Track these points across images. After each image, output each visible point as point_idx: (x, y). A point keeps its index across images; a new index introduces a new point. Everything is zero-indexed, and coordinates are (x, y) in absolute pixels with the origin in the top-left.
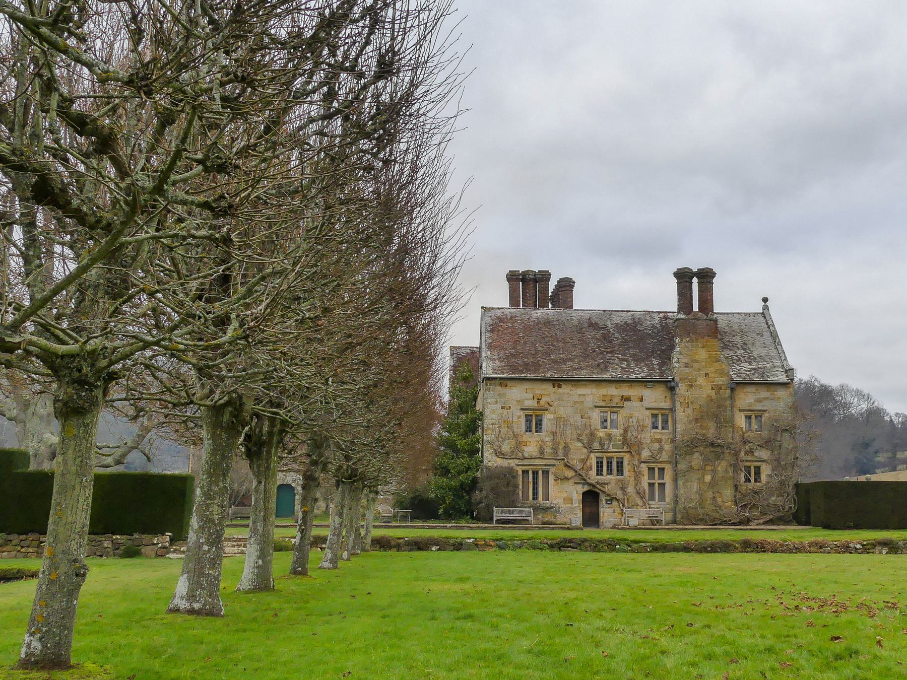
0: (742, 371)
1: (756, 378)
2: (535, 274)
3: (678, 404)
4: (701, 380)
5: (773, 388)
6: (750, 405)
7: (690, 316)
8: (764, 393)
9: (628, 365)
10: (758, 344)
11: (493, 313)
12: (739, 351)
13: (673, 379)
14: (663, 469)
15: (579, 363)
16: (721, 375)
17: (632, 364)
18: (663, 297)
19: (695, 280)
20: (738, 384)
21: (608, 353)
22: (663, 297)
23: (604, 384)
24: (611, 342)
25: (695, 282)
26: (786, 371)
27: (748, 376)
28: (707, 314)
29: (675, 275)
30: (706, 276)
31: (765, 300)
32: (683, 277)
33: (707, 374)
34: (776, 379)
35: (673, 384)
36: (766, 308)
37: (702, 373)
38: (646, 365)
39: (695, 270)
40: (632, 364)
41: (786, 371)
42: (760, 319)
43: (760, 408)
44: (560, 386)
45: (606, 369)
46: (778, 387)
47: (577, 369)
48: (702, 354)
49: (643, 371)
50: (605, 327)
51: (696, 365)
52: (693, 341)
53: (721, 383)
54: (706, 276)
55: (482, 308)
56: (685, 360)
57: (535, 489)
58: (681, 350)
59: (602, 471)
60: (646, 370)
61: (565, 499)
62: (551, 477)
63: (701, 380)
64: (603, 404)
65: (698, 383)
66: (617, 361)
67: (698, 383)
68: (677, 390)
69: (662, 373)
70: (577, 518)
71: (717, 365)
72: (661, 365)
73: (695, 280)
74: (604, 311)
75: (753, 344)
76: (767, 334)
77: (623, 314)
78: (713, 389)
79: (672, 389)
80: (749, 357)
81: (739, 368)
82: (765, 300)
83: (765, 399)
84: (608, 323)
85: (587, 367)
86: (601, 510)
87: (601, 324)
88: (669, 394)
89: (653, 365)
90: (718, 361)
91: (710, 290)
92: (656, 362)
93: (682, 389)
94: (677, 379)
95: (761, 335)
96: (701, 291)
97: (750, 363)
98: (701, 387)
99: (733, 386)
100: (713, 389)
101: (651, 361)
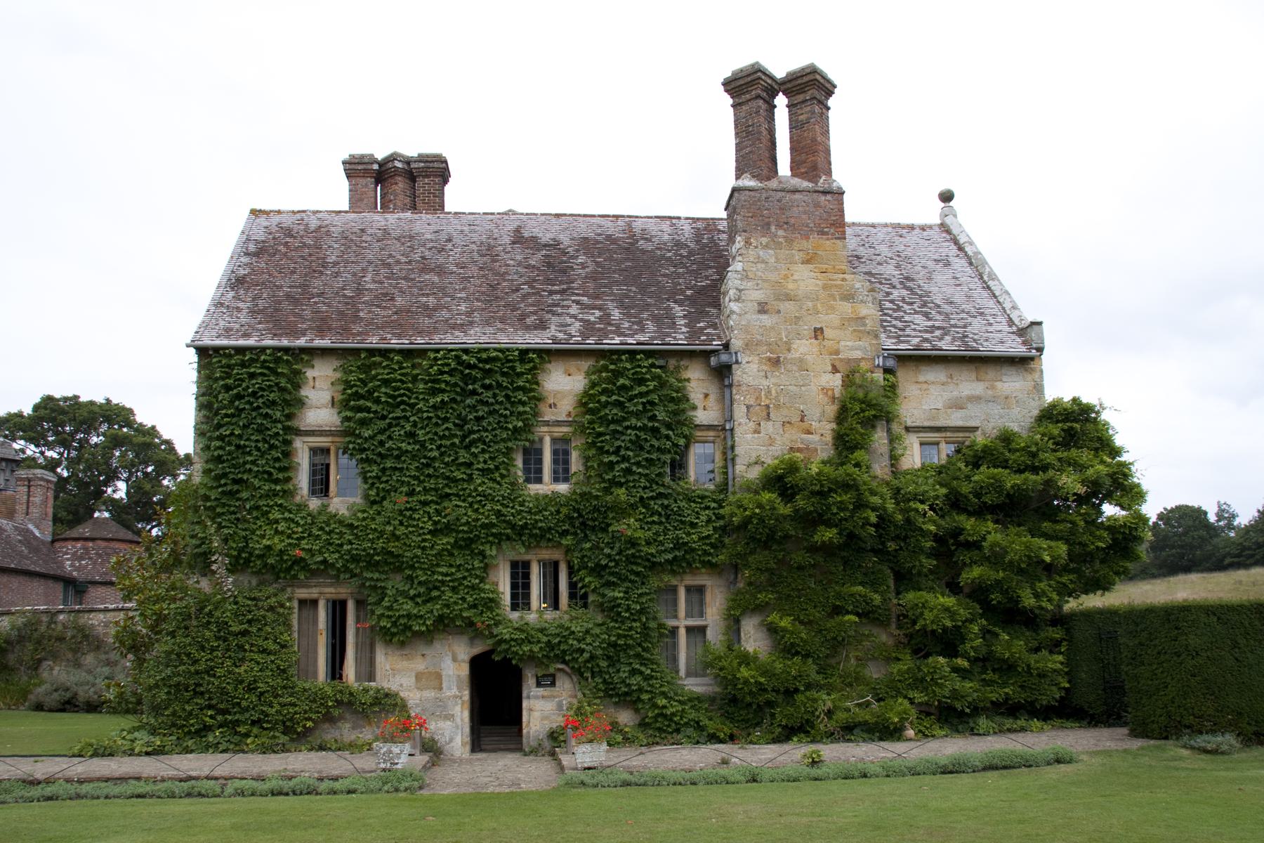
0: (908, 332)
1: (947, 345)
2: (408, 161)
3: (739, 412)
5: (991, 372)
8: (968, 385)
9: (606, 319)
11: (276, 219)
13: (726, 346)
14: (700, 590)
15: (469, 314)
17: (616, 314)
20: (903, 359)
24: (564, 271)
27: (926, 340)
31: (947, 197)
32: (749, 88)
33: (818, 332)
35: (724, 358)
37: (806, 329)
38: (656, 319)
39: (779, 73)
40: (616, 314)
41: (1022, 332)
43: (960, 423)
45: (542, 325)
47: (462, 327)
49: (641, 324)
50: (555, 244)
51: (787, 307)
53: (857, 354)
56: (758, 295)
59: (527, 596)
60: (650, 326)
61: (419, 677)
63: (804, 347)
65: (794, 355)
66: (574, 310)
67: (794, 355)
68: (738, 374)
69: (694, 334)
70: (454, 727)
71: (846, 307)
72: (691, 319)
74: (558, 216)
75: (930, 279)
76: (959, 264)
77: (607, 223)
78: (835, 370)
80: (925, 305)
81: (899, 324)
82: (947, 197)
86: (525, 704)
87: (546, 238)
89: (673, 318)
90: (849, 297)
92: (678, 310)
93: (748, 372)
94: (736, 344)
96: (794, 125)
97: (927, 316)
98: (802, 365)
99: (891, 363)
100: (835, 370)
101: (669, 309)
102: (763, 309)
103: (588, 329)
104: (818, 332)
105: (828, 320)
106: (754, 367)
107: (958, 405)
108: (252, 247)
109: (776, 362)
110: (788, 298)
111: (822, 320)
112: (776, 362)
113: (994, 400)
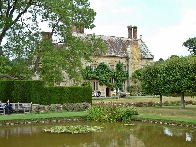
4: (135, 57)
6: (144, 64)
18: (124, 34)
19: (132, 29)
22: (124, 34)
23: (111, 57)
26: (152, 55)
28: (136, 39)
30: (135, 28)
34: (150, 58)
41: (152, 55)
44: (100, 58)
48: (135, 50)
51: (133, 53)
54: (135, 28)
56: (131, 52)
57: (94, 87)
58: (130, 49)
62: (98, 84)
63: (135, 57)
64: (111, 63)
66: (112, 51)
68: (129, 60)
70: (105, 95)
73: (132, 29)
79: (128, 60)
88: (126, 61)
90: (139, 52)
93: (130, 60)
94: (129, 56)
102: (132, 53)
110: (134, 52)
111: (137, 54)
112: (132, 59)
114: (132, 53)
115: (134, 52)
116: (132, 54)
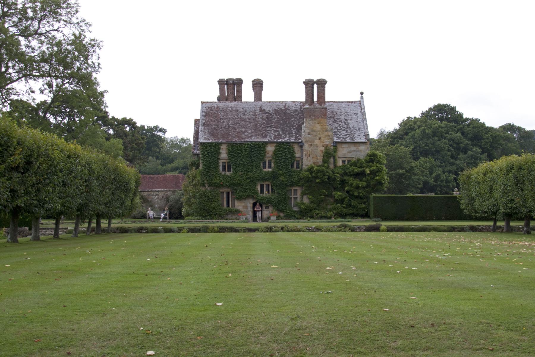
0: (341, 136)
3: (304, 155)
5: (358, 145)
6: (345, 154)
7: (312, 107)
8: (353, 148)
9: (279, 134)
10: (354, 119)
11: (207, 105)
12: (342, 124)
14: (297, 190)
15: (251, 133)
16: (328, 139)
17: (281, 133)
19: (315, 86)
21: (268, 127)
25: (315, 86)
26: (365, 136)
27: (344, 138)
28: (321, 105)
29: (304, 83)
31: (362, 93)
32: (309, 84)
35: (301, 144)
36: (362, 98)
37: (318, 138)
38: (289, 134)
39: (315, 80)
40: (281, 133)
42: (357, 104)
45: (266, 136)
46: (361, 144)
47: (249, 137)
51: (314, 133)
52: (312, 120)
53: (328, 143)
55: (202, 102)
56: (308, 131)
60: (288, 136)
63: (317, 142)
68: (304, 147)
74: (270, 102)
76: (360, 114)
81: (340, 134)
82: (362, 93)
83: (354, 151)
84: (271, 110)
85: (255, 136)
87: (267, 110)
89: (292, 133)
90: (327, 131)
91: (324, 90)
92: (294, 131)
93: (306, 147)
94: (304, 141)
95: (356, 114)
96: (318, 92)
97: (347, 131)
98: (316, 145)
102: (309, 134)
103: (275, 137)
104: (320, 139)
105: (322, 136)
106: (307, 146)
107: (350, 152)
108: (204, 114)
109: (311, 145)
110: (314, 131)
111: (321, 136)
113: (358, 151)
114: (309, 134)
115: (314, 131)
116: (310, 136)
